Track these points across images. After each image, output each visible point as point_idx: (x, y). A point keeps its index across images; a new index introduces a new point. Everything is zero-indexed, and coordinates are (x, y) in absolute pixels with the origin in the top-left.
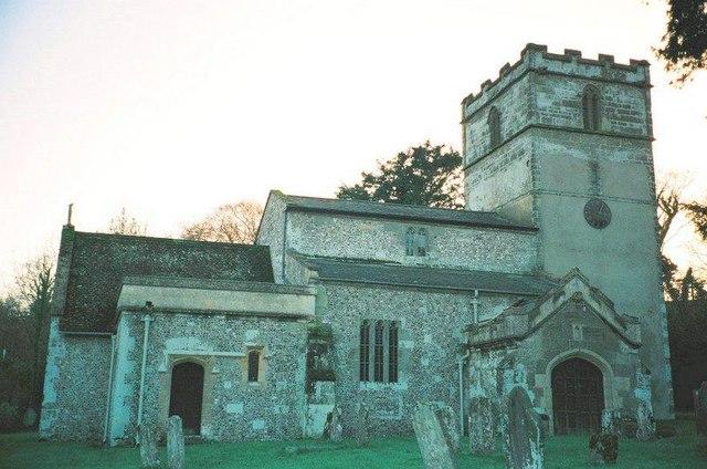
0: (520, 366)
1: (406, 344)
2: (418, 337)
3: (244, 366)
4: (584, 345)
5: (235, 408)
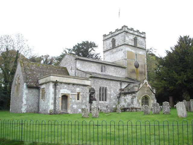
0: (136, 98)
1: (108, 92)
2: (110, 91)
3: (76, 96)
4: (147, 93)
5: (75, 106)
